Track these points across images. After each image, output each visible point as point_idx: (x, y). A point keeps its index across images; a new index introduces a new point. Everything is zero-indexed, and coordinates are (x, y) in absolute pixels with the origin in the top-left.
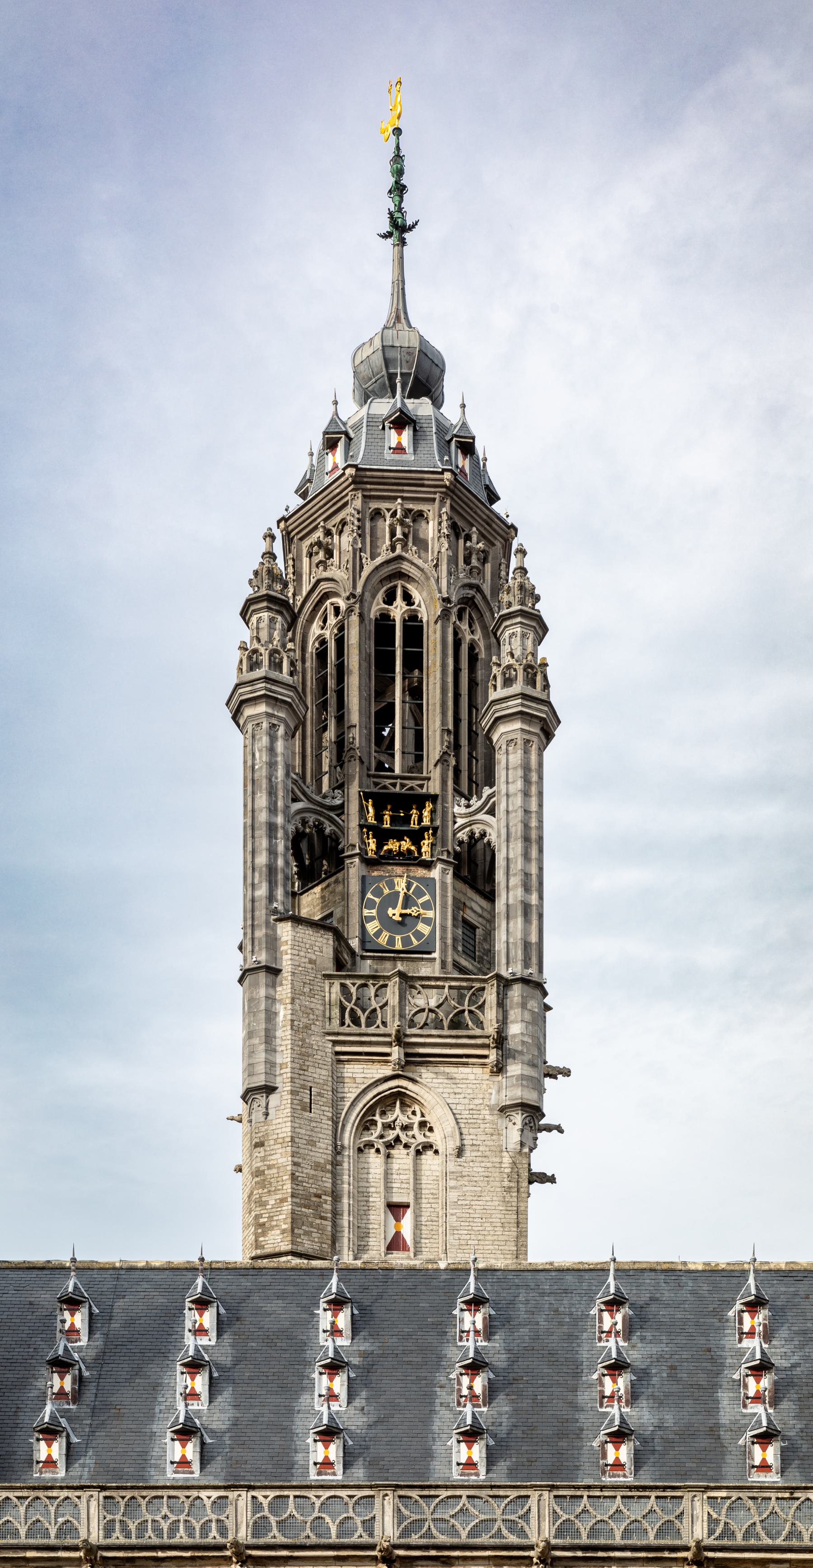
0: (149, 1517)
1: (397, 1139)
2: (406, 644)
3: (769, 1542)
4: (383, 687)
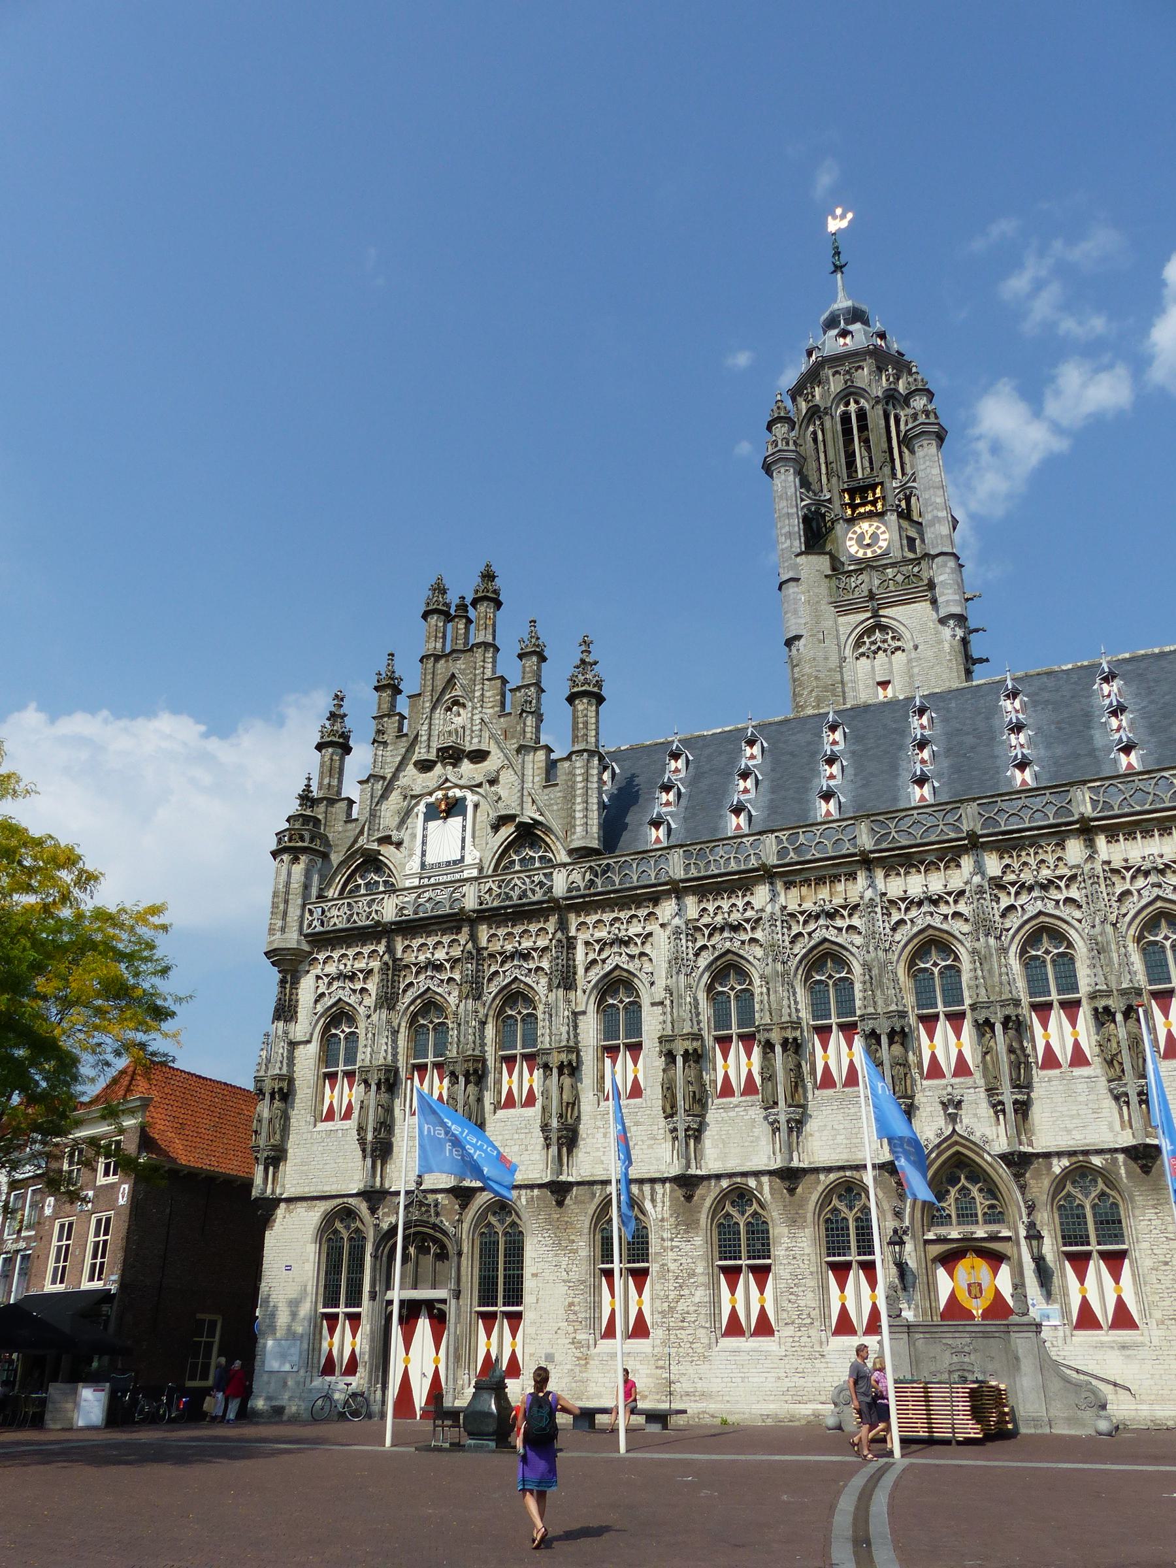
0: (711, 858)
1: (879, 648)
2: (858, 421)
3: (1138, 808)
4: (849, 441)
